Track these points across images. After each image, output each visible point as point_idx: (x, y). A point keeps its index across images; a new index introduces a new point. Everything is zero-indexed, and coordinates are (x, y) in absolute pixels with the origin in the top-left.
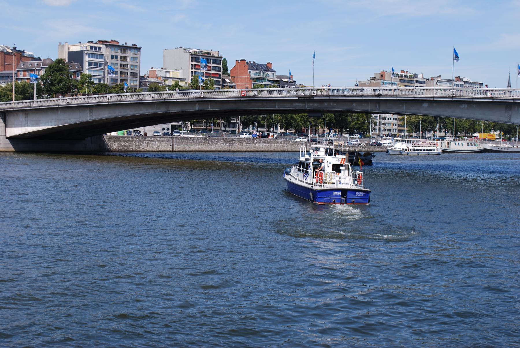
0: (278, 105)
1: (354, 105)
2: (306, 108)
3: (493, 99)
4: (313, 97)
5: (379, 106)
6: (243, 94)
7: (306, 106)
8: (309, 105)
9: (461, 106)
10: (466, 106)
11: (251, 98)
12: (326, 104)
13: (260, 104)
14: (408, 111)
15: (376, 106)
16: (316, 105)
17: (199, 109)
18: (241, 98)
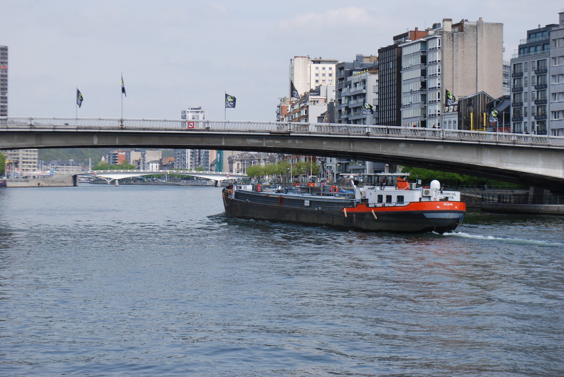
0: (225, 141)
1: (325, 143)
2: (264, 146)
3: (480, 142)
4: (289, 133)
5: (353, 145)
6: (190, 126)
7: (264, 144)
8: (267, 141)
9: (437, 148)
10: (441, 147)
11: (204, 130)
12: (290, 141)
13: (199, 139)
14: (385, 151)
15: (350, 145)
16: (277, 142)
17: (98, 143)
18: (187, 130)
